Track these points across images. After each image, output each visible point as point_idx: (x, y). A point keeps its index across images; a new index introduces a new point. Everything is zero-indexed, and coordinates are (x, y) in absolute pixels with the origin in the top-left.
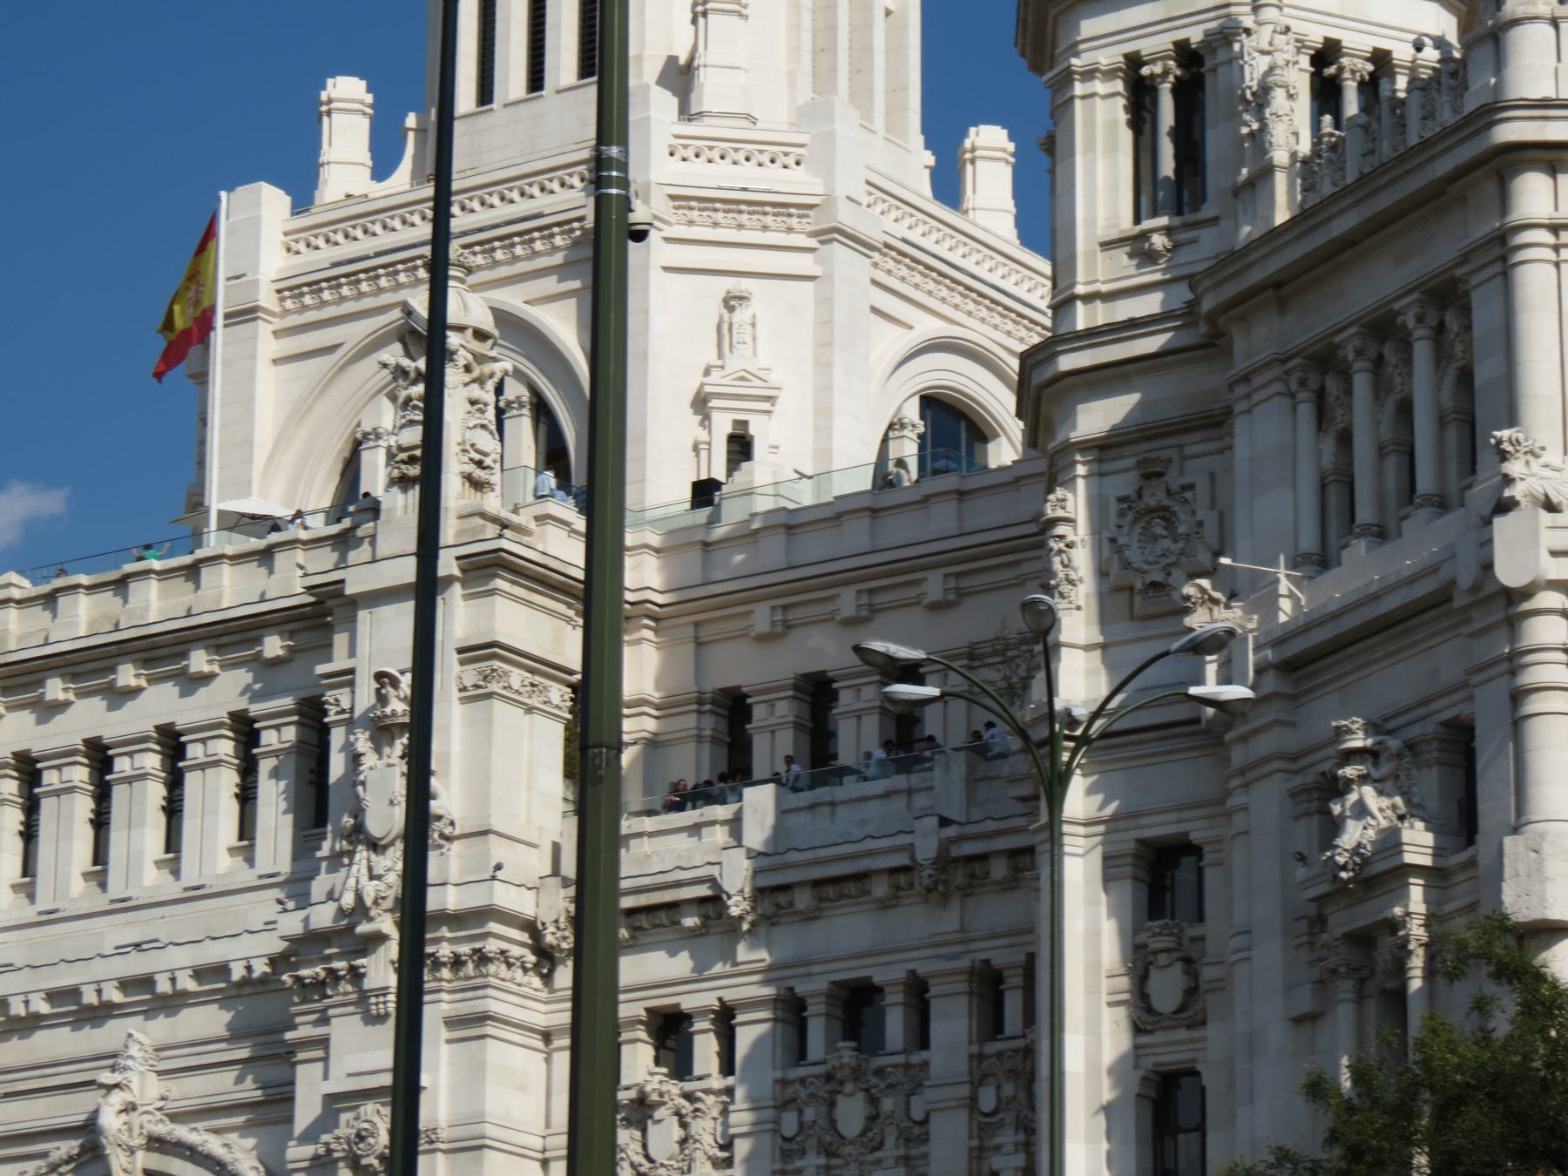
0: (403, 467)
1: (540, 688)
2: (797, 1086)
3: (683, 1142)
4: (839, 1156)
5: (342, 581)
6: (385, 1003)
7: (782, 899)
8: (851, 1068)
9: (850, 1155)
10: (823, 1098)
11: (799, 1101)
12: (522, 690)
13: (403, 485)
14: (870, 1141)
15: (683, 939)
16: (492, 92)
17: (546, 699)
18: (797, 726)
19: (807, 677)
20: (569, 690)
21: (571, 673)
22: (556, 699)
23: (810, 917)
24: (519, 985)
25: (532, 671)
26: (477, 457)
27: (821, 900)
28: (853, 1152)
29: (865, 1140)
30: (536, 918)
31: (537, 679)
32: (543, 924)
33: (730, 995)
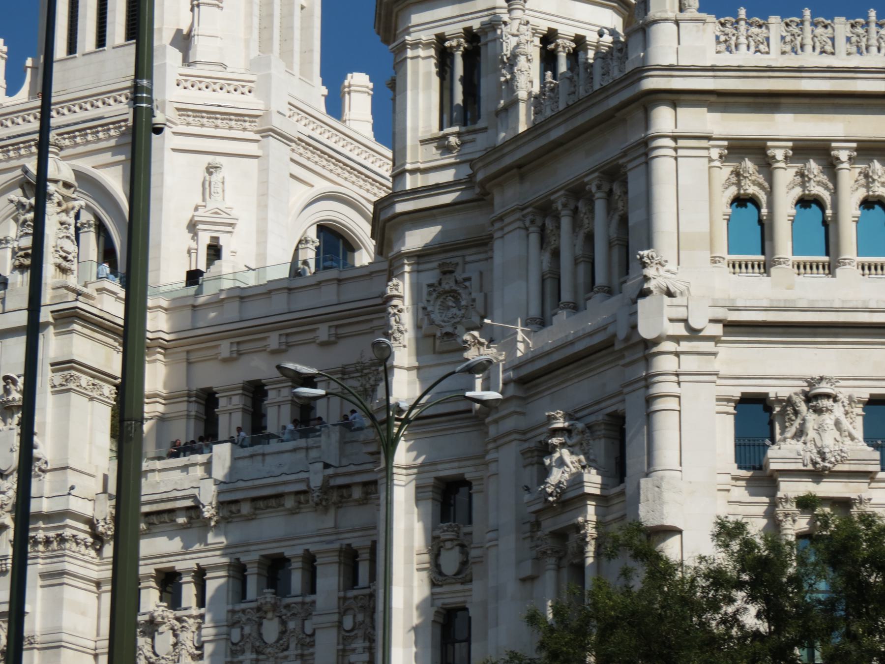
2: (240, 614)
3: (175, 645)
4: (264, 654)
6: (6, 564)
7: (234, 508)
9: (270, 653)
12: (87, 387)
18: (244, 410)
20: (114, 388)
21: (116, 378)
23: (249, 518)
24: (83, 555)
25: (94, 377)
26: (64, 254)
27: (256, 509)
28: (272, 651)
29: (279, 645)
31: (96, 381)
32: (97, 520)
33: (203, 562)
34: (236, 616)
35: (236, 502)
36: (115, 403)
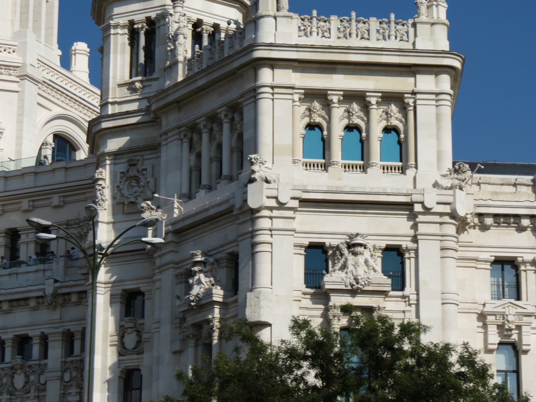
4: (14, 395)
8: (20, 365)
10: (9, 375)
15: (30, 311)
18: (6, 246)
19: (10, 229)
27: (12, 307)
29: (24, 390)
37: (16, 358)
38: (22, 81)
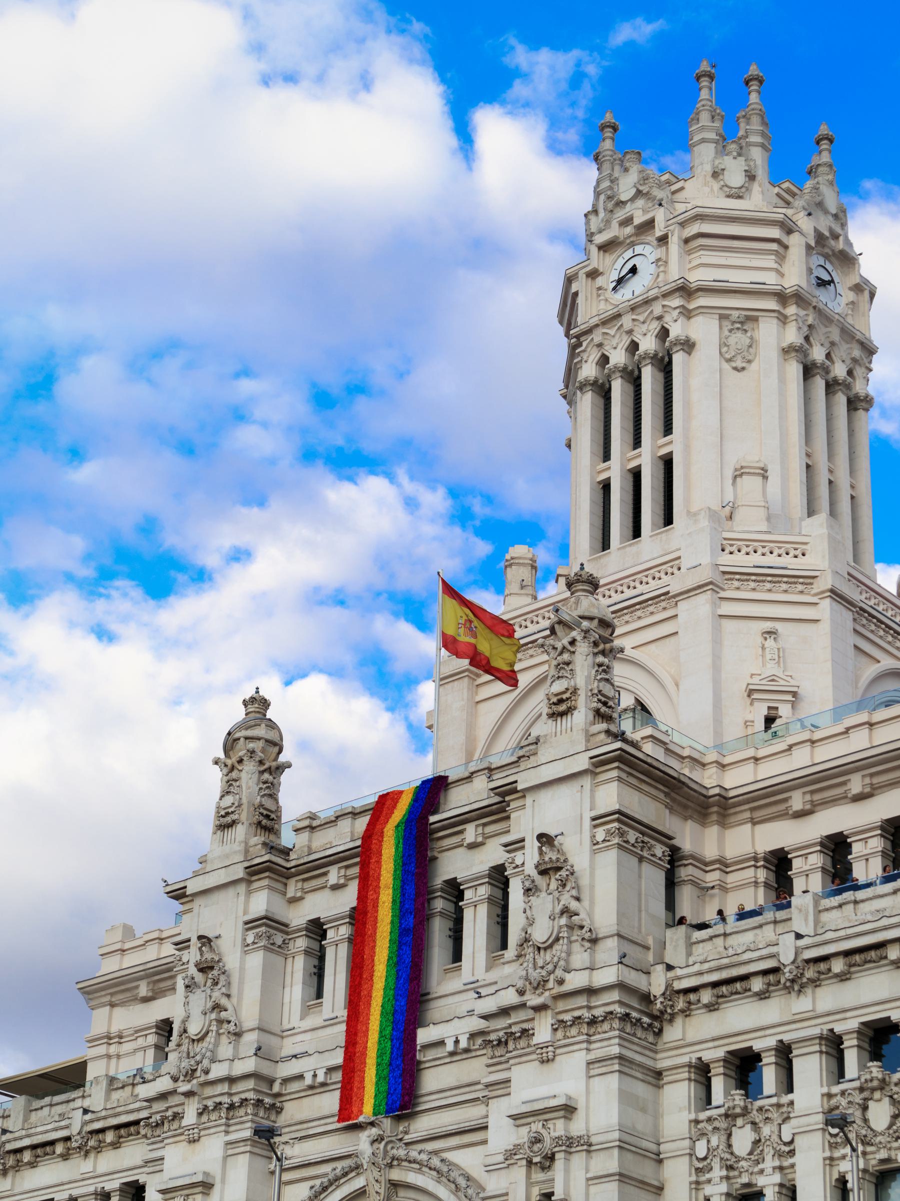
0: (553, 707)
1: (649, 845)
2: (839, 1097)
3: (757, 1142)
4: (872, 1145)
5: (516, 782)
6: (547, 1053)
7: (823, 966)
8: (879, 1080)
9: (880, 1143)
10: (858, 1104)
11: (841, 1107)
12: (636, 844)
13: (554, 719)
14: (895, 1132)
16: (610, 454)
17: (652, 853)
18: (824, 870)
19: (829, 837)
20: (668, 850)
21: (670, 838)
22: (658, 853)
23: (843, 977)
24: (640, 1039)
25: (643, 834)
26: (603, 699)
27: (851, 966)
28: (883, 1141)
29: (891, 1131)
30: (650, 993)
31: (646, 839)
32: (655, 996)
33: (786, 1038)
34: (833, 1102)
35: (825, 958)
36: (669, 867)
37: (869, 1068)
38: (822, 601)
